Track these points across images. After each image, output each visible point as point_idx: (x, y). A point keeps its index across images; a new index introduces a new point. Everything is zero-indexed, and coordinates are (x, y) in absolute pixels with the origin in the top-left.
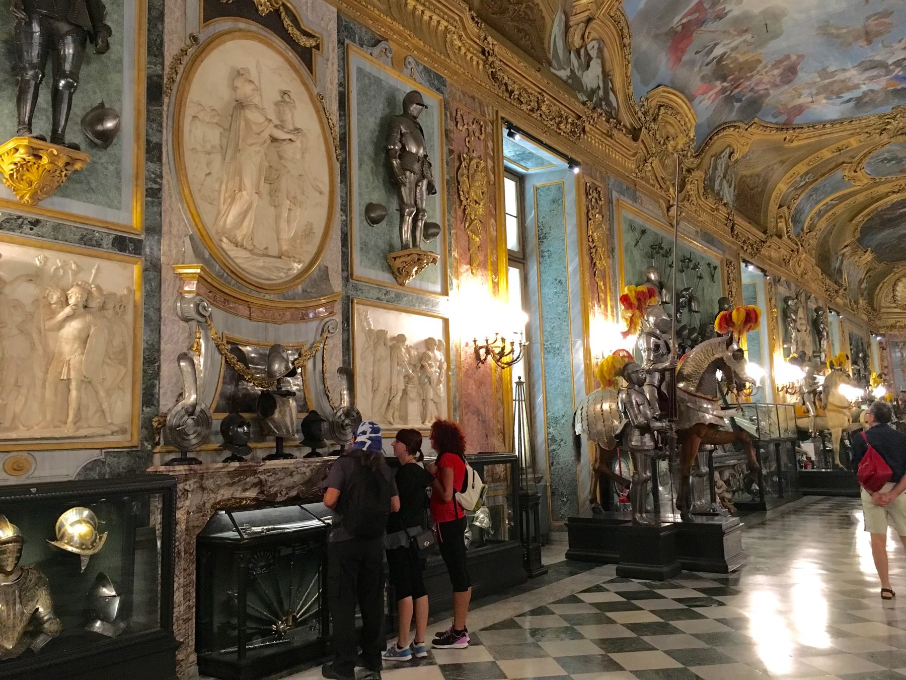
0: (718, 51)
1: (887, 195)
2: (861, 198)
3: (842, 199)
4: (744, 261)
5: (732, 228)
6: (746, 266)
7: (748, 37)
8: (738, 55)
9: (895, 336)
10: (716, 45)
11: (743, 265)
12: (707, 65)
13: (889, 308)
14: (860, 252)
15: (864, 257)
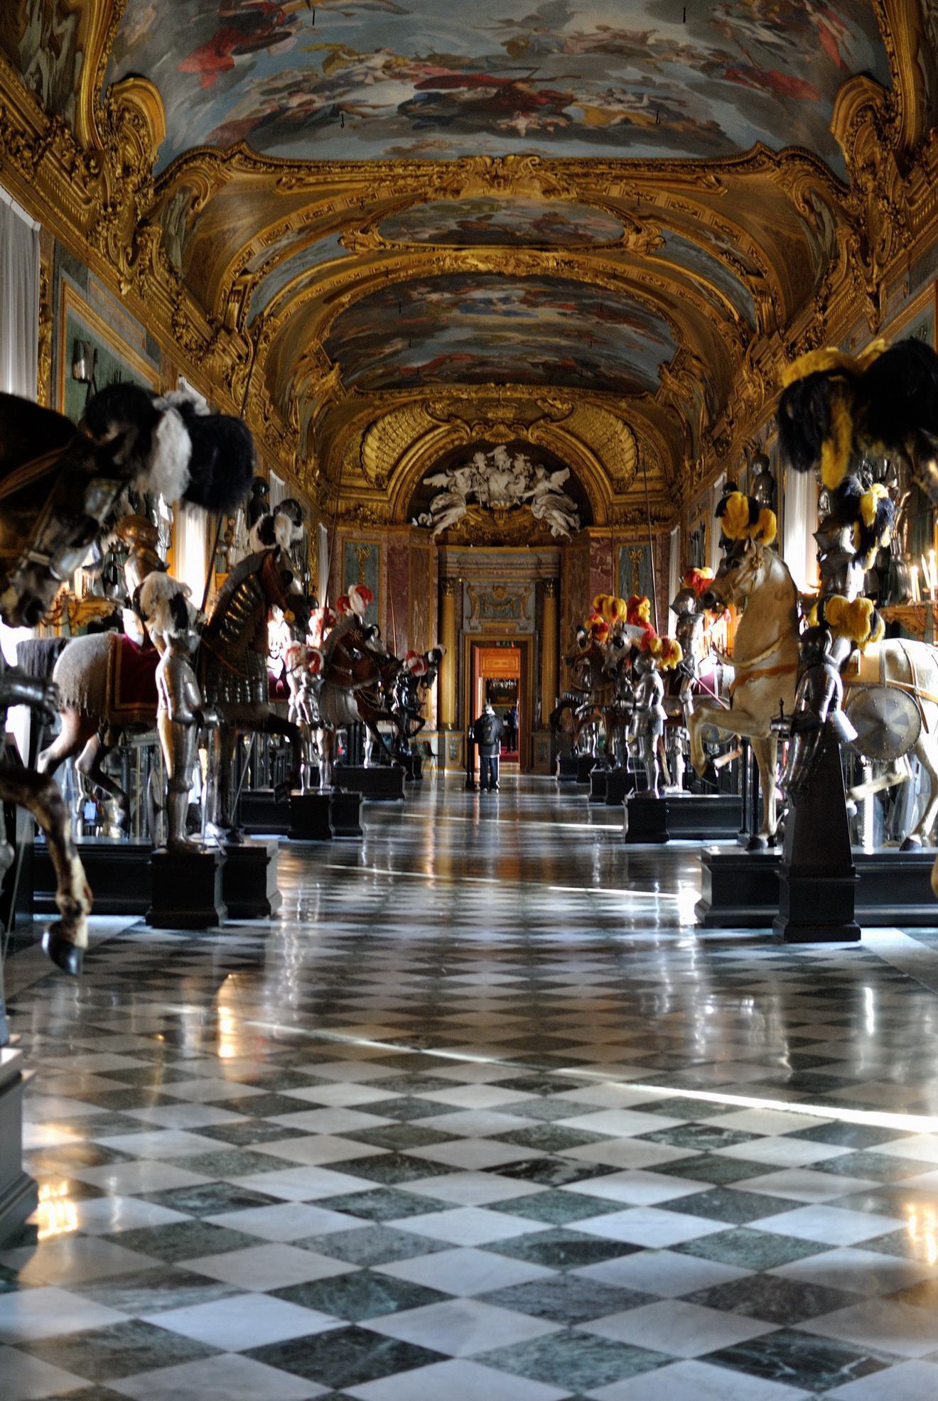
0: (766, 35)
7: (719, 14)
8: (755, 9)
10: (761, 43)
12: (793, 44)
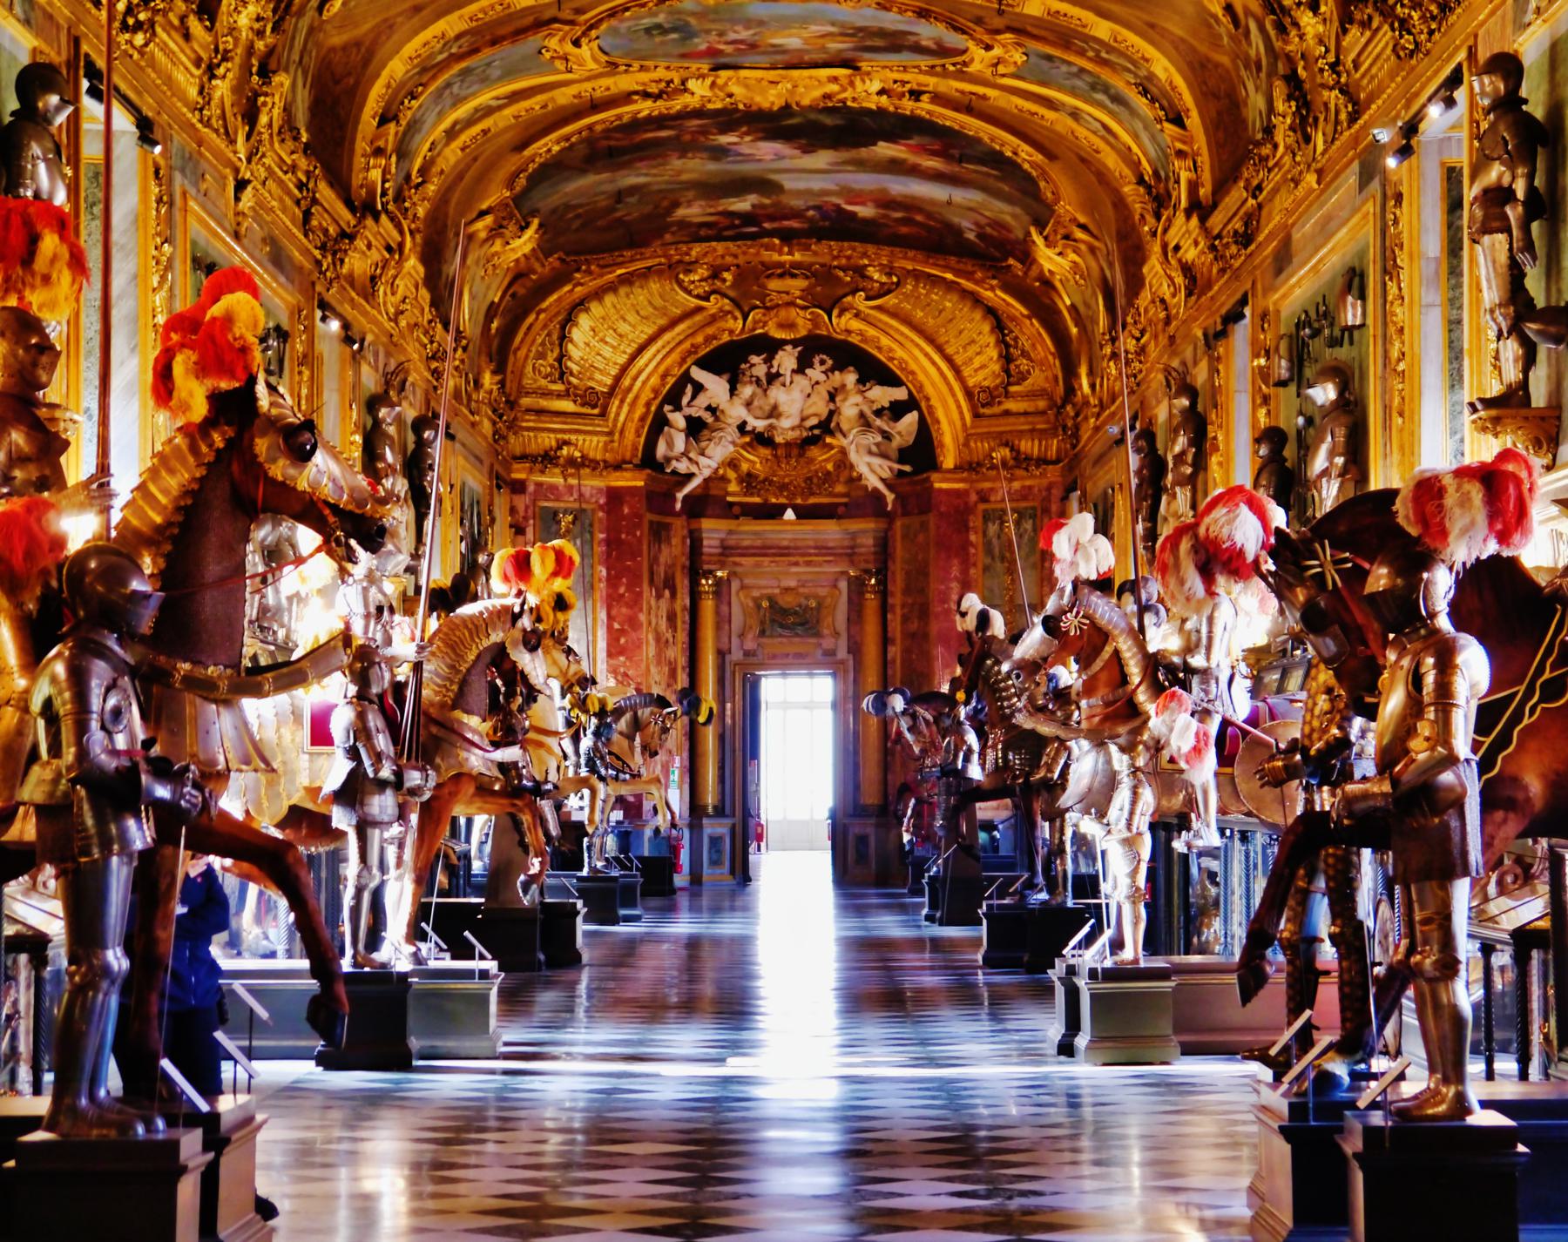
1: (627, 98)
2: (564, 97)
3: (515, 97)
4: (323, 305)
5: (307, 215)
6: (324, 319)
9: (553, 488)
11: (319, 314)
13: (547, 394)
14: (512, 227)
15: (516, 243)
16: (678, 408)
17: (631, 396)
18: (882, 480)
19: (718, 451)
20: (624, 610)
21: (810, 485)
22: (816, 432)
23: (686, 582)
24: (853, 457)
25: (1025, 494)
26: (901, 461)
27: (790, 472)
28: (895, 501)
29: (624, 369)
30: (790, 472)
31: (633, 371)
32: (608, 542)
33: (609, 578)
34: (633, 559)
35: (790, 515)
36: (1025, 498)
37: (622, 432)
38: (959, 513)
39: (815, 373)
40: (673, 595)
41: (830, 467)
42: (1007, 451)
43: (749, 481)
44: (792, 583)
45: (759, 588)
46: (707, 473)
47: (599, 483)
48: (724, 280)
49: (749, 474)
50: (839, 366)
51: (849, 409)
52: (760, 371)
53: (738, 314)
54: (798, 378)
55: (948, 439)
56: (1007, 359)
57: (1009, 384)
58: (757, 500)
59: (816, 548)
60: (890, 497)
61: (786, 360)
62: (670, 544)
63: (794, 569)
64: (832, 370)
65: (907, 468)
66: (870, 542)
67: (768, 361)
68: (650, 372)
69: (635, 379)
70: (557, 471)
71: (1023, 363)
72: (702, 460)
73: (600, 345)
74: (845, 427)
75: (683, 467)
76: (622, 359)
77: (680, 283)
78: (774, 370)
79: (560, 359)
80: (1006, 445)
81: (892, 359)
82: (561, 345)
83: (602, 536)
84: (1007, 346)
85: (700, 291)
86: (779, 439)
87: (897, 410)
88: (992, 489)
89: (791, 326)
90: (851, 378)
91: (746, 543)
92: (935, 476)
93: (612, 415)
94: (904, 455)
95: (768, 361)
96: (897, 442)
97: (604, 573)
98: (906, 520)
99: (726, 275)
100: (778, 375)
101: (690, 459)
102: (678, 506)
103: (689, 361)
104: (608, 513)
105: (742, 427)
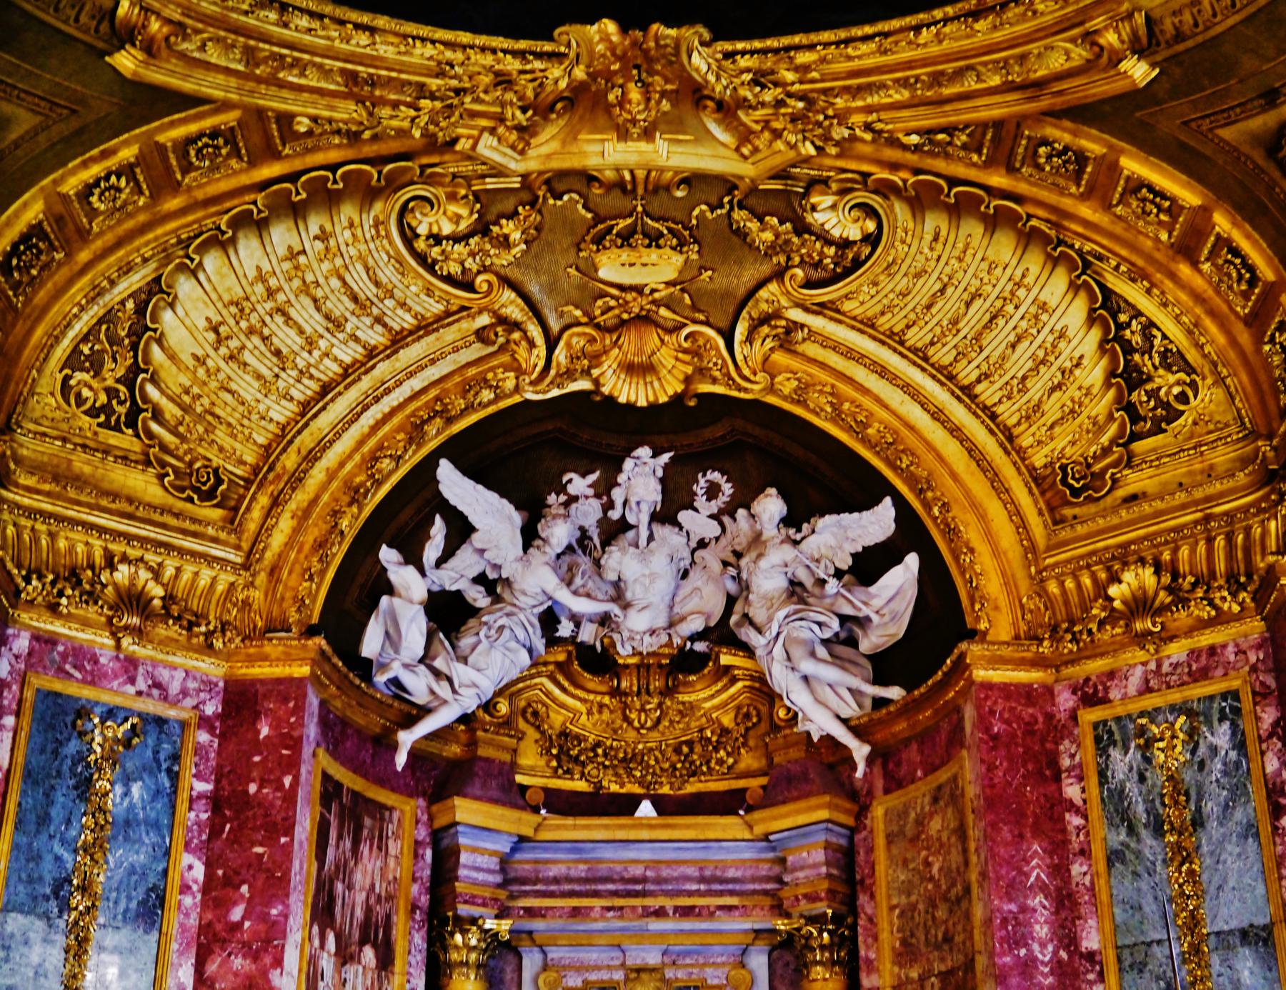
9: (81, 656)
16: (413, 557)
17: (300, 498)
18: (845, 721)
19: (492, 662)
20: (238, 962)
21: (690, 757)
22: (700, 647)
23: (419, 939)
24: (781, 678)
25: (1205, 664)
26: (878, 680)
27: (652, 730)
28: (870, 760)
29: (284, 436)
30: (652, 730)
31: (306, 440)
32: (216, 802)
33: (206, 889)
34: (270, 841)
35: (646, 809)
36: (1202, 675)
37: (274, 571)
38: (1032, 742)
39: (698, 521)
40: (385, 961)
41: (727, 721)
42: (1148, 576)
43: (564, 749)
44: (652, 958)
45: (580, 968)
46: (469, 702)
47: (213, 668)
48: (505, 243)
49: (564, 734)
50: (743, 499)
51: (768, 578)
52: (589, 513)
53: (535, 331)
54: (663, 531)
55: (992, 586)
56: (1127, 377)
57: (1135, 437)
58: (581, 786)
59: (702, 880)
60: (860, 751)
61: (642, 478)
62: (382, 847)
63: (655, 925)
64: (730, 510)
65: (895, 693)
66: (819, 856)
67: (604, 490)
68: (347, 440)
69: (311, 457)
70: (91, 612)
71: (1168, 383)
72: (460, 672)
73: (228, 369)
74: (758, 614)
75: (419, 685)
76: (281, 412)
77: (409, 236)
78: (615, 515)
79: (129, 380)
80: (1142, 561)
81: (859, 429)
82: (134, 347)
83: (202, 787)
84: (1128, 349)
85: (454, 269)
86: (624, 652)
87: (868, 566)
88: (1111, 675)
89: (640, 369)
90: (771, 506)
91: (554, 871)
92: (974, 650)
93: (252, 527)
94: (884, 667)
95: (604, 490)
96: (870, 642)
97: (199, 871)
98: (896, 800)
99: (511, 229)
100: (623, 526)
101: (437, 674)
102: (401, 759)
103: (436, 436)
104: (223, 737)
105: (549, 619)
